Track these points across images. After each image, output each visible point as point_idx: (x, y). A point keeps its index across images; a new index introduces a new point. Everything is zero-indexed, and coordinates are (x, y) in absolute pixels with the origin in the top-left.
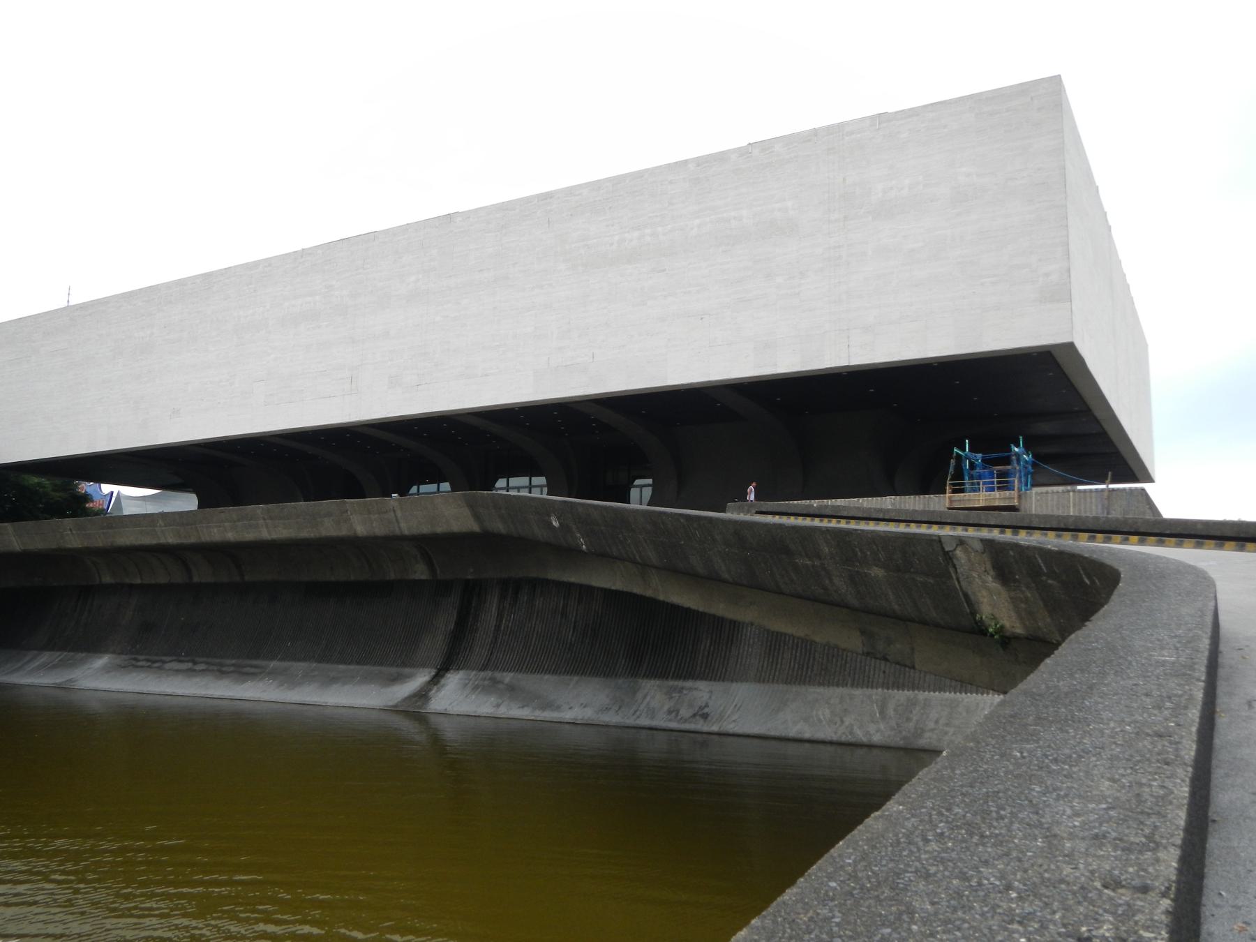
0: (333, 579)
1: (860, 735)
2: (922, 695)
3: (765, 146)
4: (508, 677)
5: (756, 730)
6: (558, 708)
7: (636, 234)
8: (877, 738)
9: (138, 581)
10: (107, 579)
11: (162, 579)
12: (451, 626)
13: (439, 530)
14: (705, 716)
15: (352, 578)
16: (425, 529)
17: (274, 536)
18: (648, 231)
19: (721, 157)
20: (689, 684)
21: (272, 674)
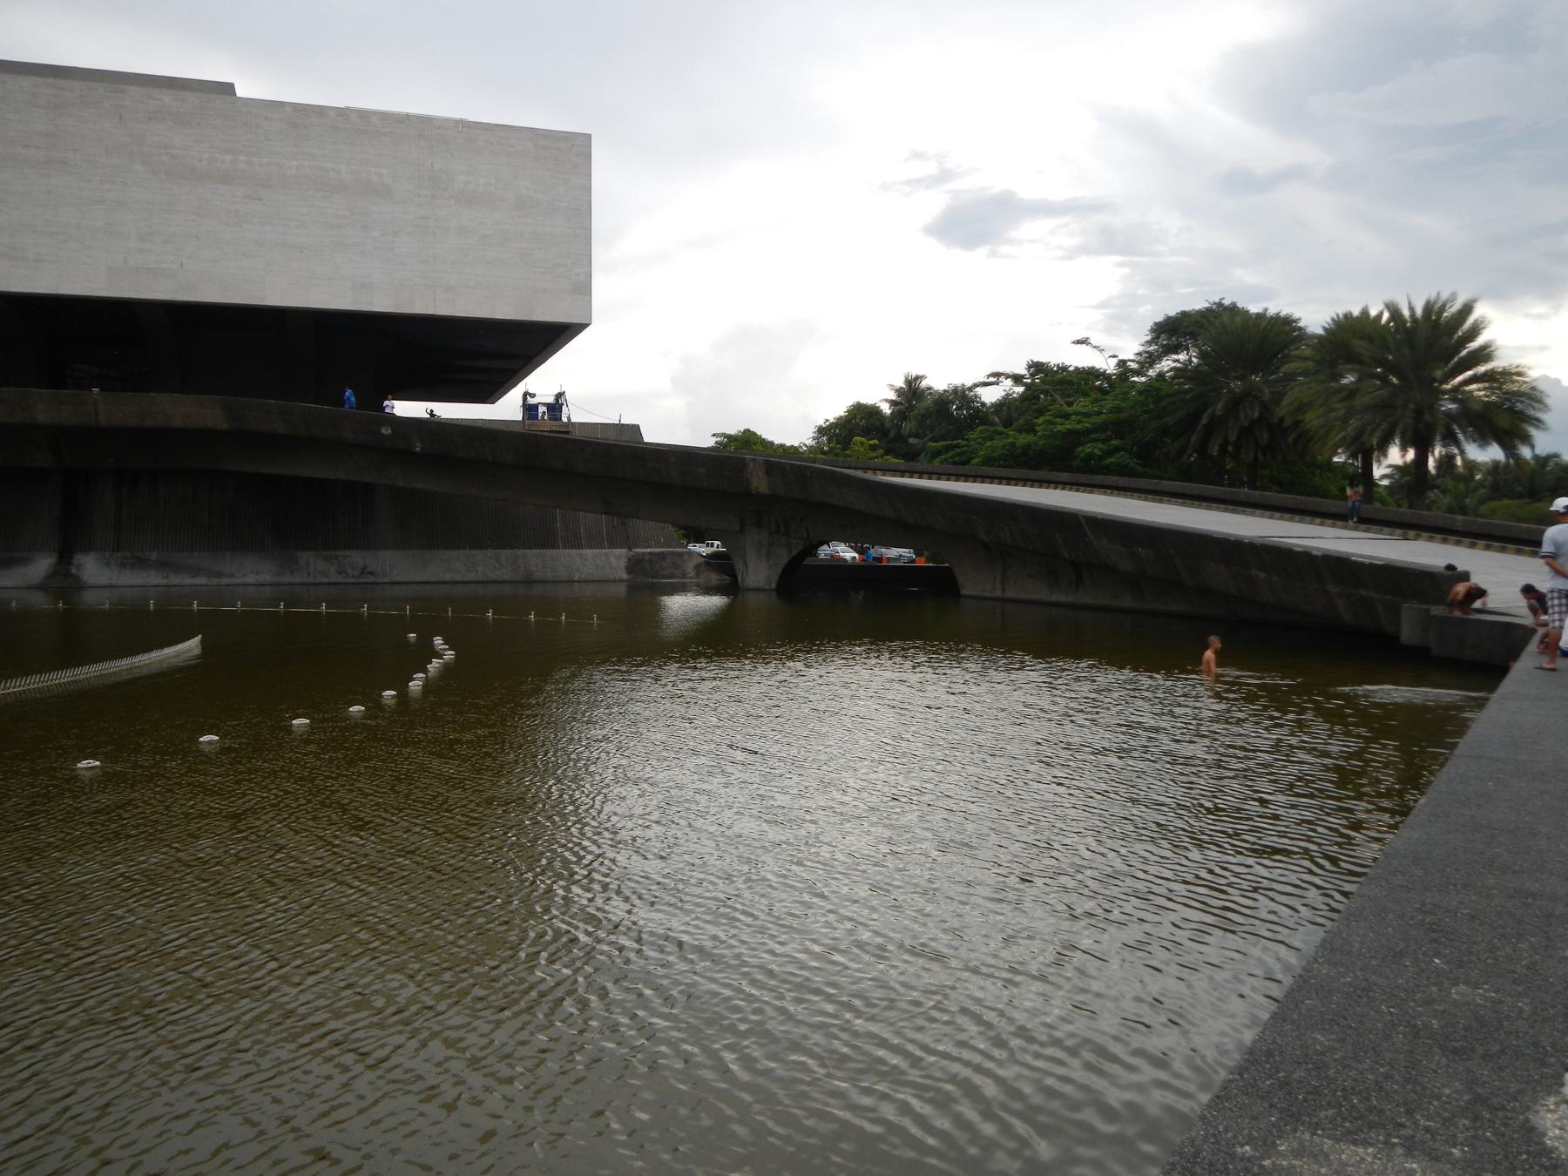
1: (493, 576)
2: (520, 552)
3: (364, 115)
4: (154, 556)
5: (418, 579)
6: (232, 576)
7: (229, 157)
8: (506, 577)
14: (372, 573)
18: (242, 158)
20: (341, 553)
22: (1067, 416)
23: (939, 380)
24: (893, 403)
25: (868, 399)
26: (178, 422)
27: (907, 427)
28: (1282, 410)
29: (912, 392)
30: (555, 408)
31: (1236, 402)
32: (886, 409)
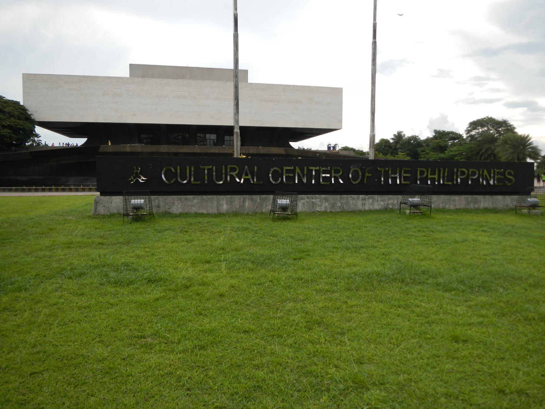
3: (297, 86)
13: (269, 153)
16: (266, 153)
17: (229, 152)
19: (289, 86)
22: (452, 151)
23: (408, 134)
24: (393, 139)
25: (385, 138)
26: (274, 153)
27: (398, 146)
28: (495, 152)
29: (399, 137)
30: (334, 147)
31: (487, 149)
32: (391, 141)
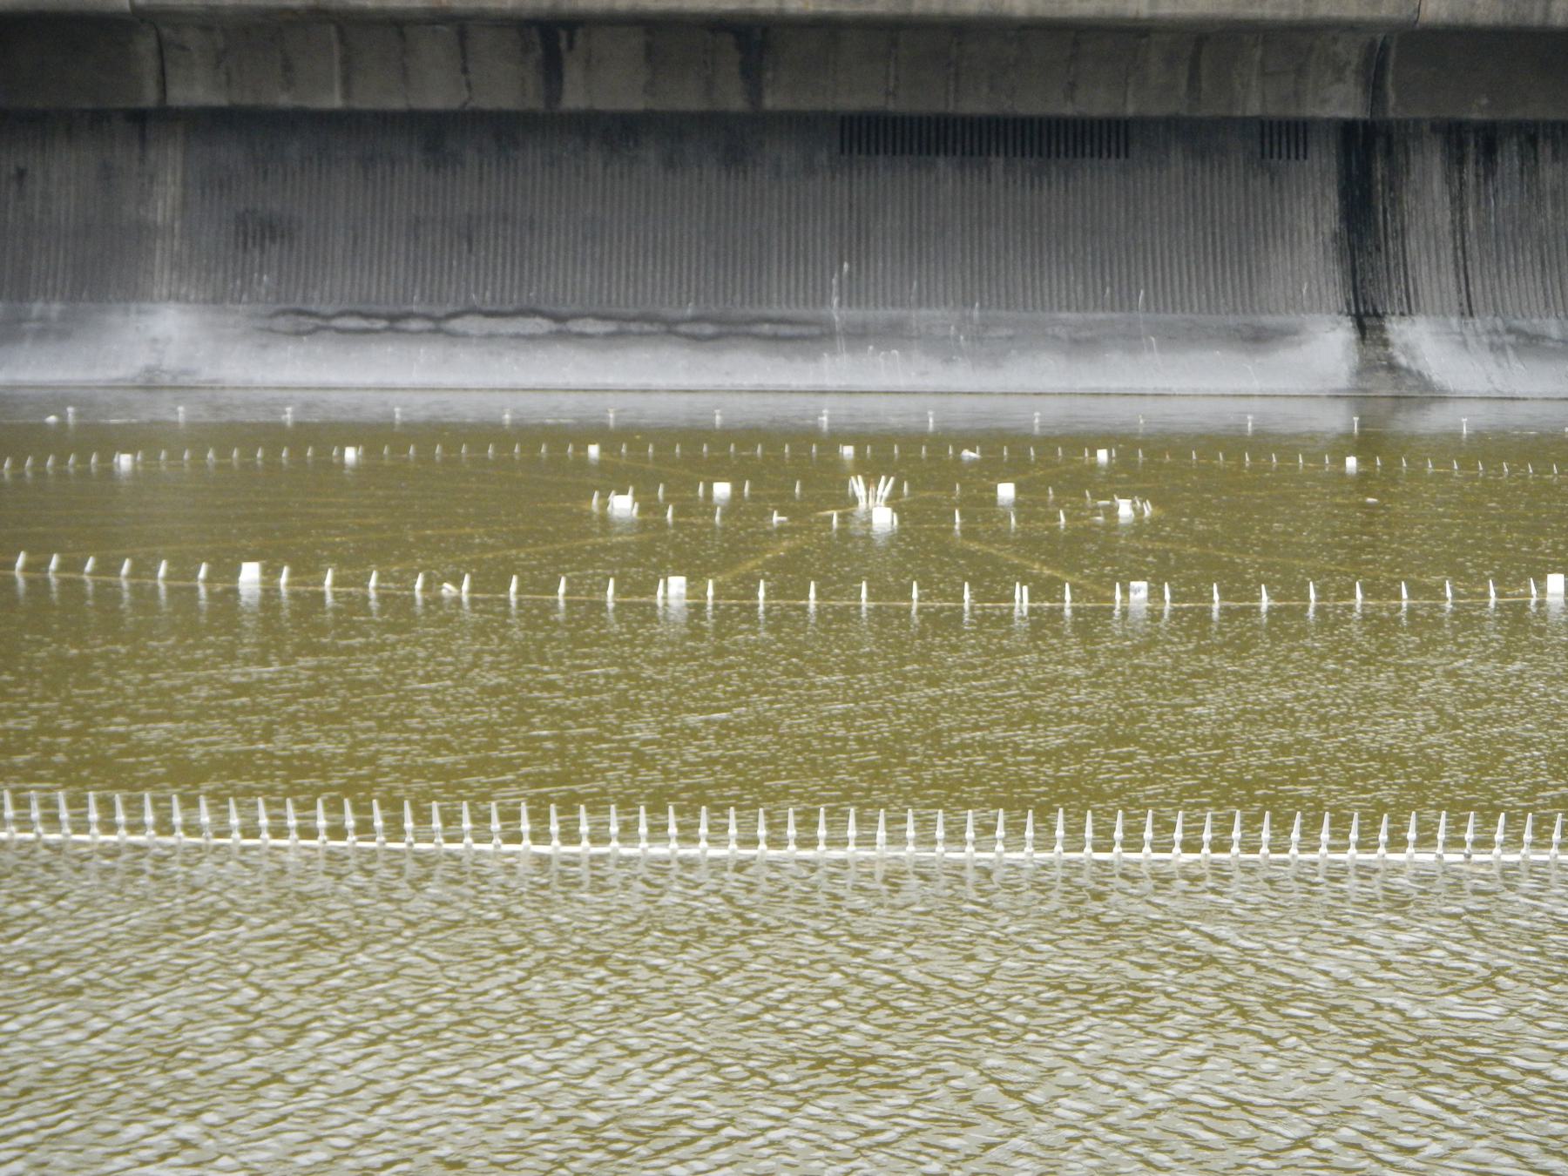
0: (1069, 110)
9: (336, 101)
10: (195, 90)
11: (438, 92)
12: (1331, 219)
15: (1130, 110)
21: (859, 336)
